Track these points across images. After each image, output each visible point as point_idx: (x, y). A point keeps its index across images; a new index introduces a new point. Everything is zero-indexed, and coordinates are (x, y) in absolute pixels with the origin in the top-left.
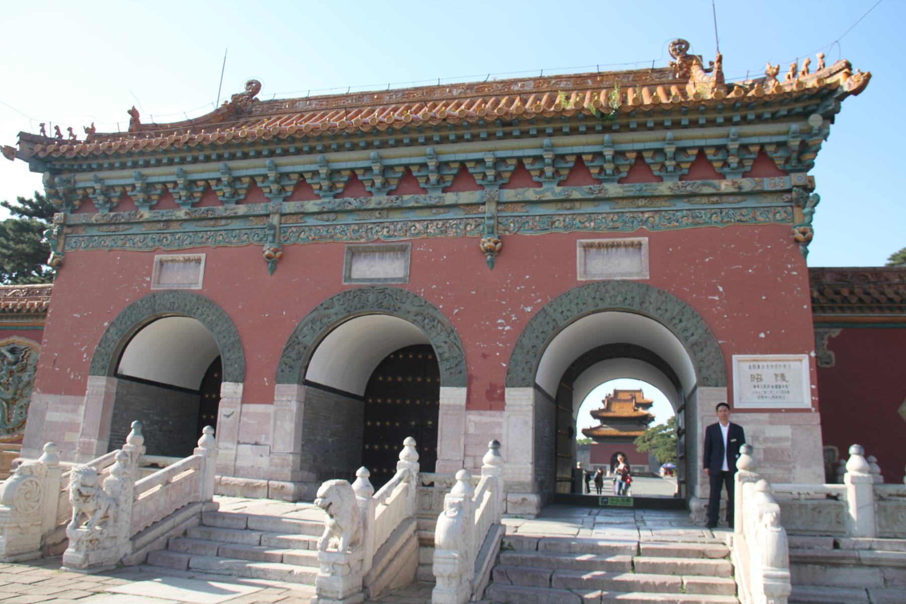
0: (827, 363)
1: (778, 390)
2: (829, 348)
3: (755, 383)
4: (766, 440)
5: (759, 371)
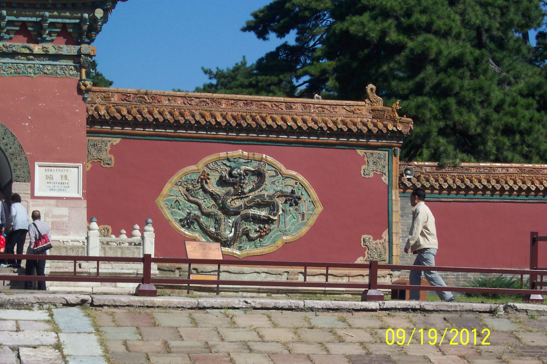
0: (108, 164)
1: (62, 185)
2: (111, 152)
3: (49, 180)
4: (53, 216)
5: (51, 173)
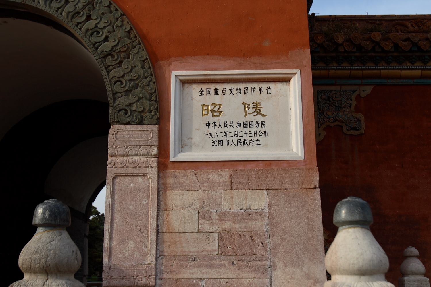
0: (355, 129)
1: (248, 129)
3: (210, 118)
4: (223, 217)
